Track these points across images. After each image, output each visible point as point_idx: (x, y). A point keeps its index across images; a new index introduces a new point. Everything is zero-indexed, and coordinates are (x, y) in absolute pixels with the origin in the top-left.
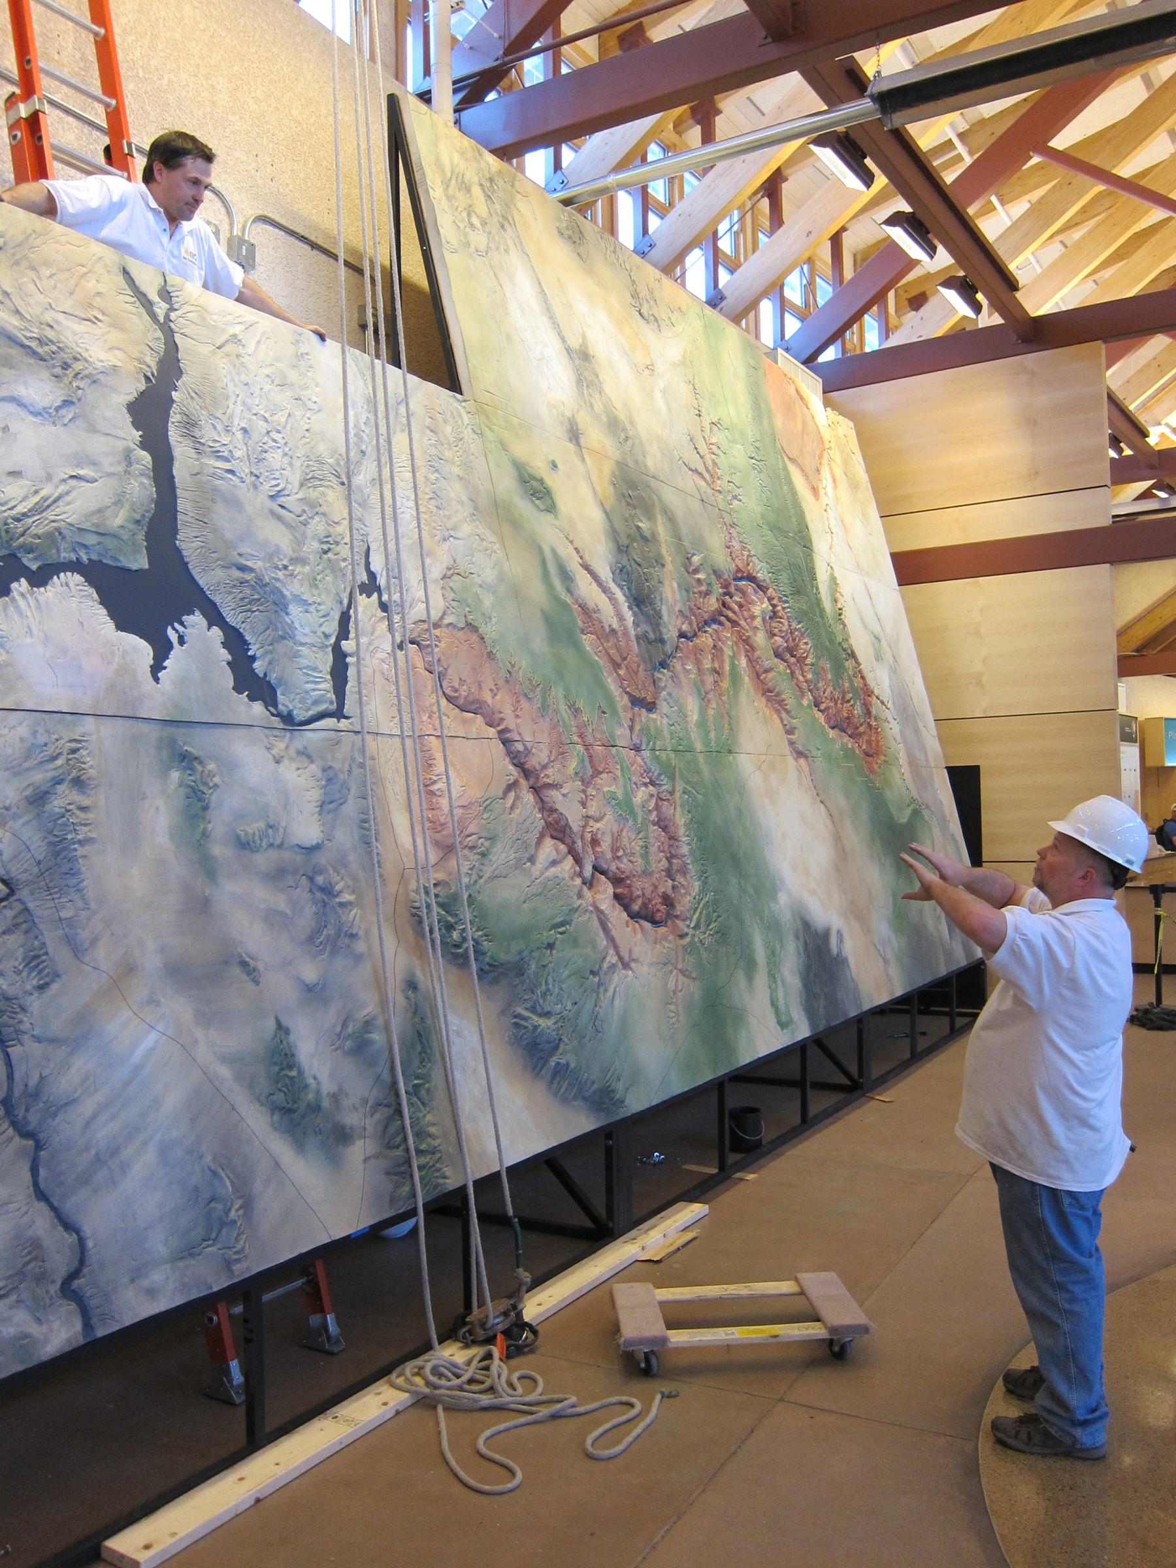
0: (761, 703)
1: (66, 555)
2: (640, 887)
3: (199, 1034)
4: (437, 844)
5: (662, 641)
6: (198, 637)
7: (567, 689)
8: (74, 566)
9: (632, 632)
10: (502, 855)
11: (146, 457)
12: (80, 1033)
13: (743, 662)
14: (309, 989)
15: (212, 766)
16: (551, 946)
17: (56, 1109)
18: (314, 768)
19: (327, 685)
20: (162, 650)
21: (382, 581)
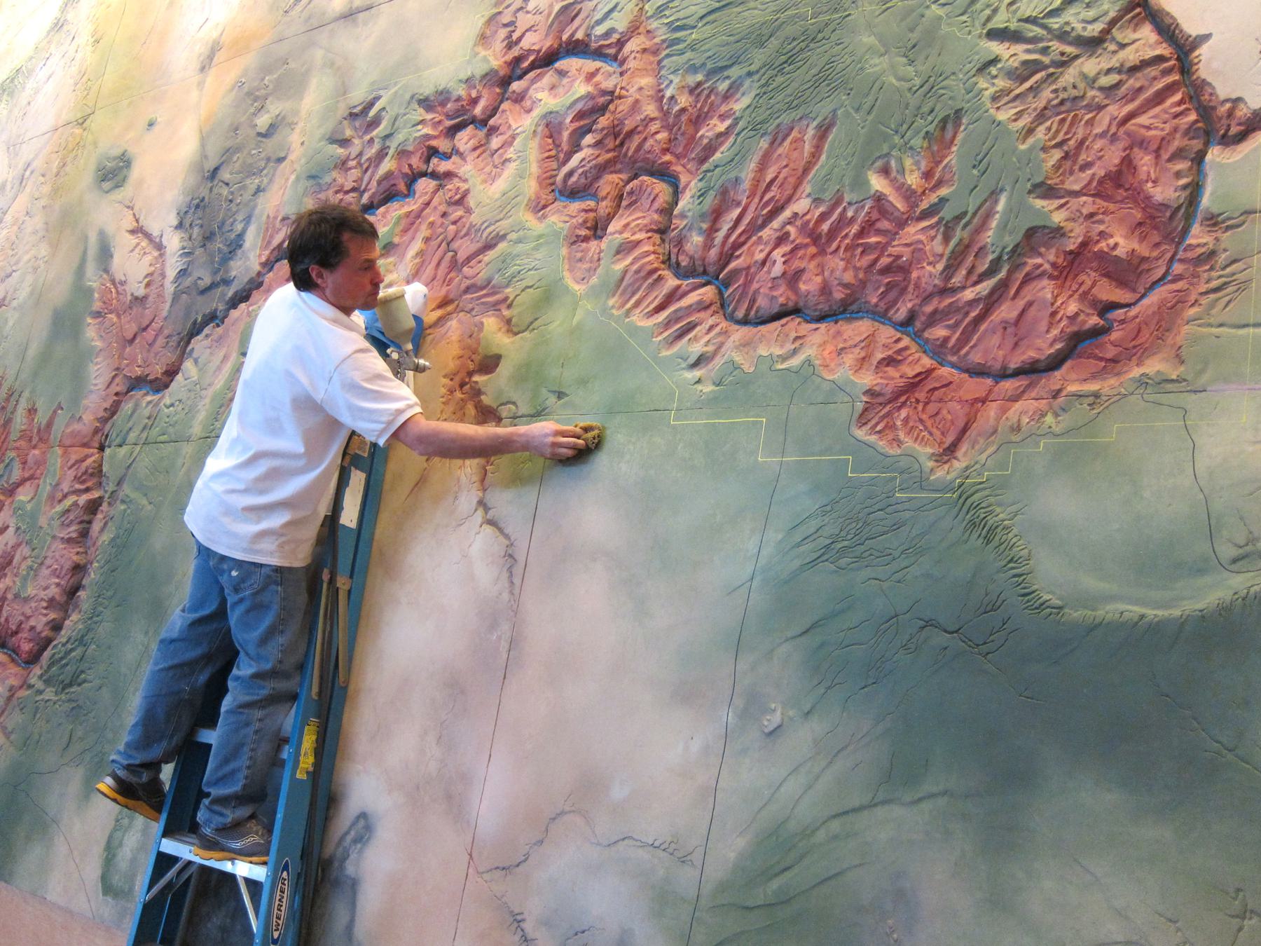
9: (170, 288)
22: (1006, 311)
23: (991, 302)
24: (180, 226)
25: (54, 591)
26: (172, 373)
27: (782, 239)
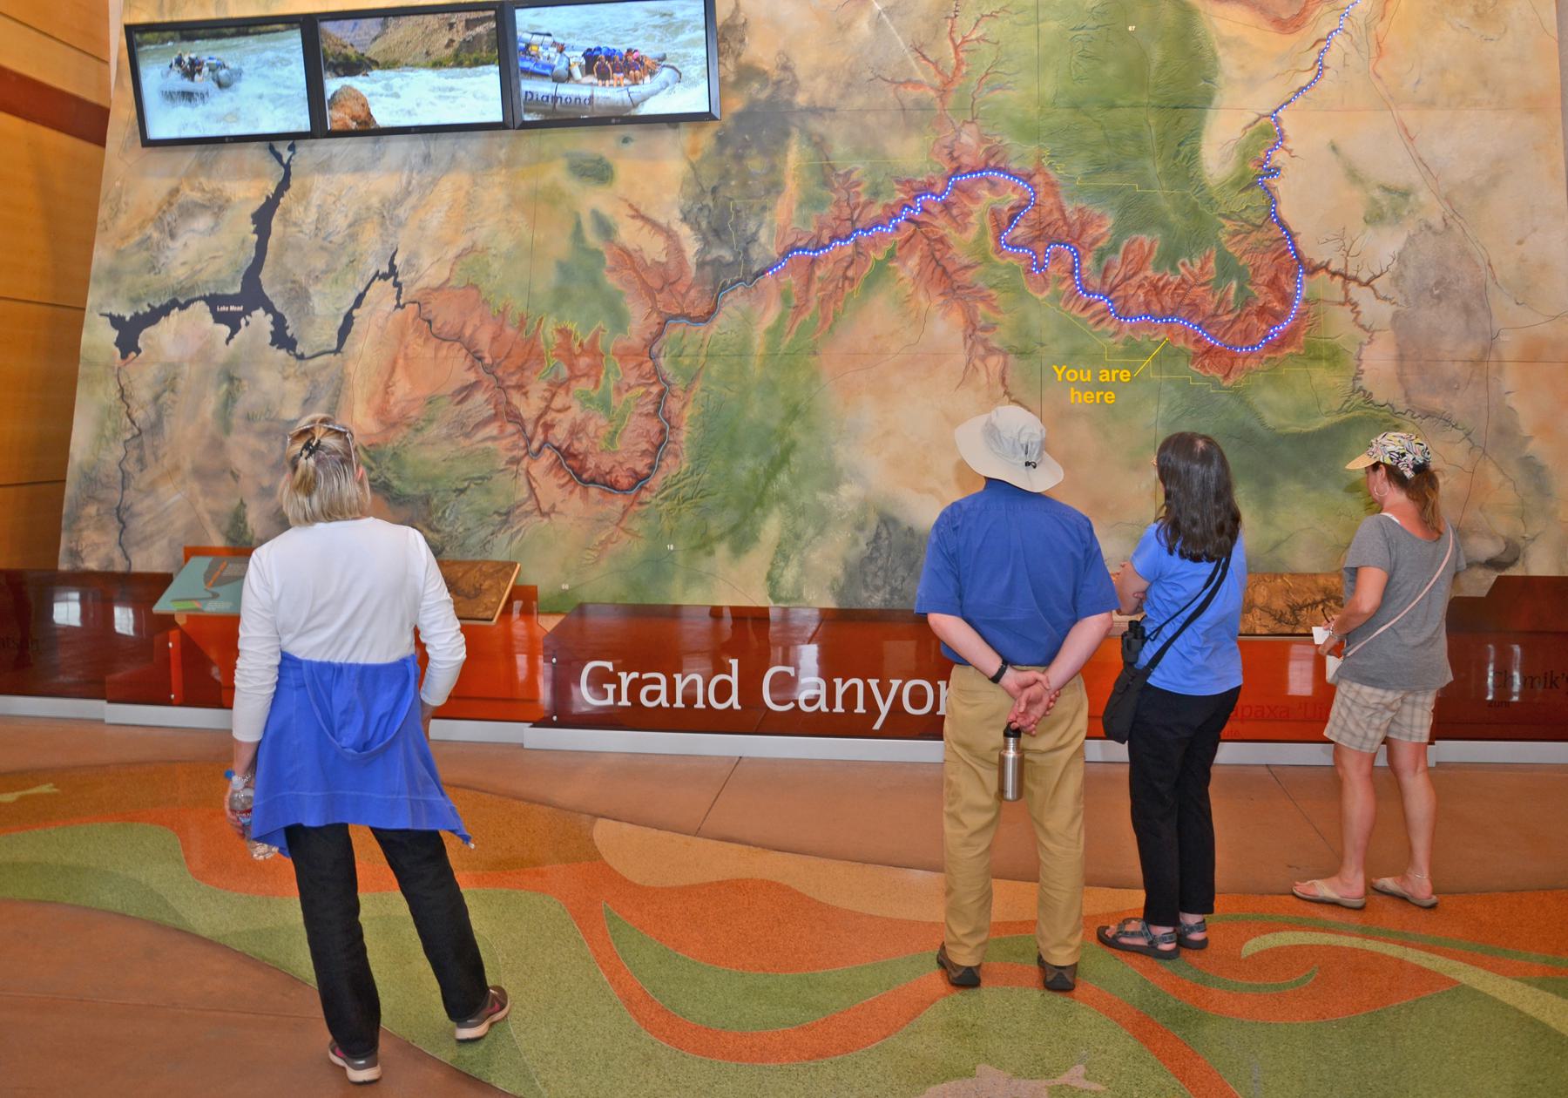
0: (929, 302)
1: (197, 295)
2: (591, 463)
3: (201, 499)
4: (382, 422)
5: (748, 260)
6: (261, 321)
7: (560, 319)
8: (204, 298)
10: (433, 431)
11: (255, 237)
12: (152, 488)
13: (913, 262)
14: (263, 489)
15: (245, 383)
16: (462, 491)
17: (132, 516)
18: (307, 382)
19: (329, 336)
20: (235, 328)
21: (399, 269)
22: (1239, 326)
23: (1234, 322)
24: (685, 219)
25: (644, 446)
26: (711, 313)
27: (1140, 286)
